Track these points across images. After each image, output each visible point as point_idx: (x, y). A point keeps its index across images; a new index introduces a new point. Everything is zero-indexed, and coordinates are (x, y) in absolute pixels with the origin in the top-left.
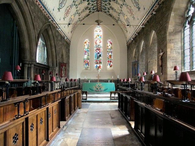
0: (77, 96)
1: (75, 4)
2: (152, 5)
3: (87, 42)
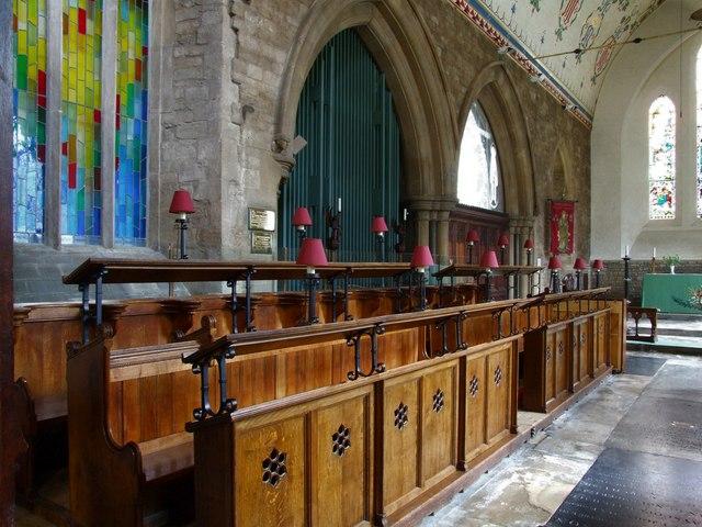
0: (607, 325)
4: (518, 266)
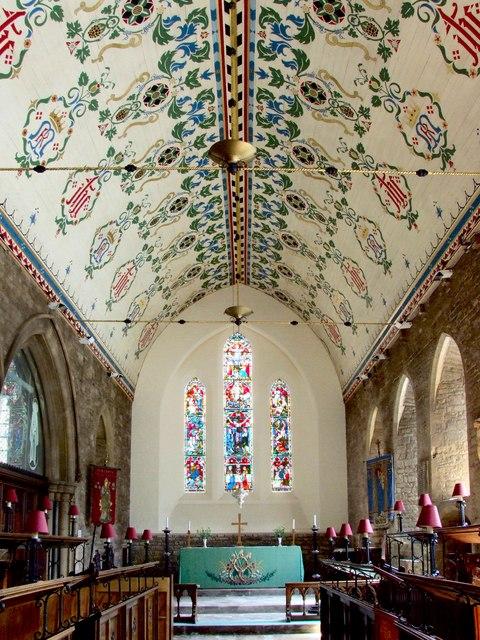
0: (155, 606)
1: (150, 257)
2: (438, 249)
3: (195, 390)
4: (57, 536)
